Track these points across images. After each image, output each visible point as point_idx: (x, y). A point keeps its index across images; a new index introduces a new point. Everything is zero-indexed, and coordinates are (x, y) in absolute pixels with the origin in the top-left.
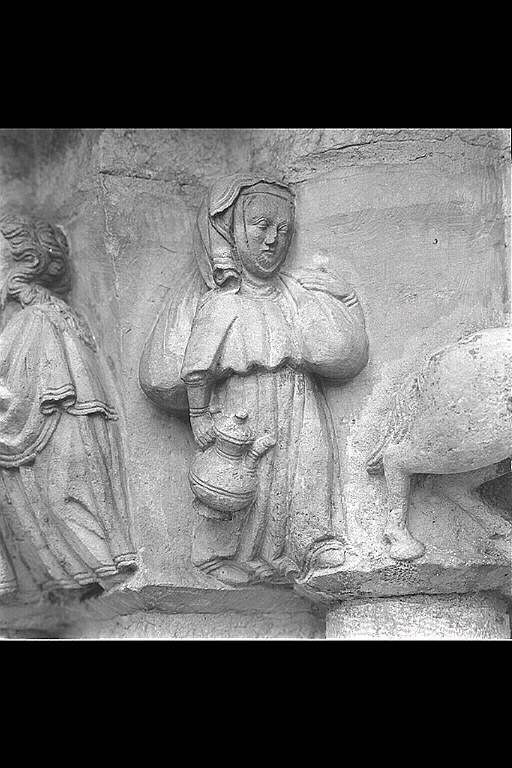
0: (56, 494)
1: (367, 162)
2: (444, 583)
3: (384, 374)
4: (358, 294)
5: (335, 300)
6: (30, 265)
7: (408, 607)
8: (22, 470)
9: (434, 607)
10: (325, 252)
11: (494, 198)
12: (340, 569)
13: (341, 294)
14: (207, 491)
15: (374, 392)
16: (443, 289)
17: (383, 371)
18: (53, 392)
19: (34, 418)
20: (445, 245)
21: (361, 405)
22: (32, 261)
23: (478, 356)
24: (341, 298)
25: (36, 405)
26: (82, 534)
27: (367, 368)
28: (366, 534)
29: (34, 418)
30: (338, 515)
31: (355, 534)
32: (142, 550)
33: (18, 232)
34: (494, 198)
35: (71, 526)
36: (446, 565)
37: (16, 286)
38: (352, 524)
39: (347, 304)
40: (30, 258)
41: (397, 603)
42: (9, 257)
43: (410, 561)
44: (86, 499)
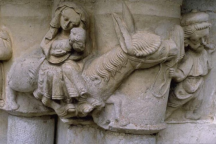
1: (14, 3)
2: (26, 115)
3: (15, 59)
4: (11, 38)
5: (4, 40)
7: (19, 118)
9: (25, 119)
10: (5, 25)
11: (49, 14)
12: (2, 108)
13: (6, 39)
15: (13, 65)
16: (31, 39)
17: (15, 59)
20: (33, 27)
21: (10, 67)
23: (23, 66)
24: (6, 39)
27: (11, 59)
28: (9, 100)
30: (3, 95)
31: (7, 99)
34: (49, 14)
36: (24, 112)
38: (7, 97)
39: (7, 41)
41: (16, 117)
43: (15, 110)
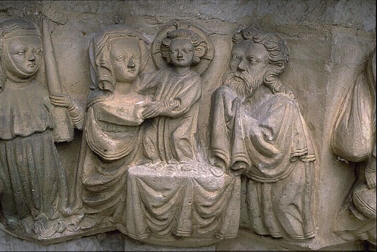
0: (285, 200)
6: (280, 69)
8: (266, 185)
14: (372, 212)
18: (300, 151)
19: (285, 163)
22: (281, 66)
25: (288, 157)
26: (292, 220)
29: (285, 163)
32: (318, 228)
33: (276, 48)
35: (288, 216)
37: (270, 79)
40: (281, 64)
42: (266, 61)
44: (300, 204)
